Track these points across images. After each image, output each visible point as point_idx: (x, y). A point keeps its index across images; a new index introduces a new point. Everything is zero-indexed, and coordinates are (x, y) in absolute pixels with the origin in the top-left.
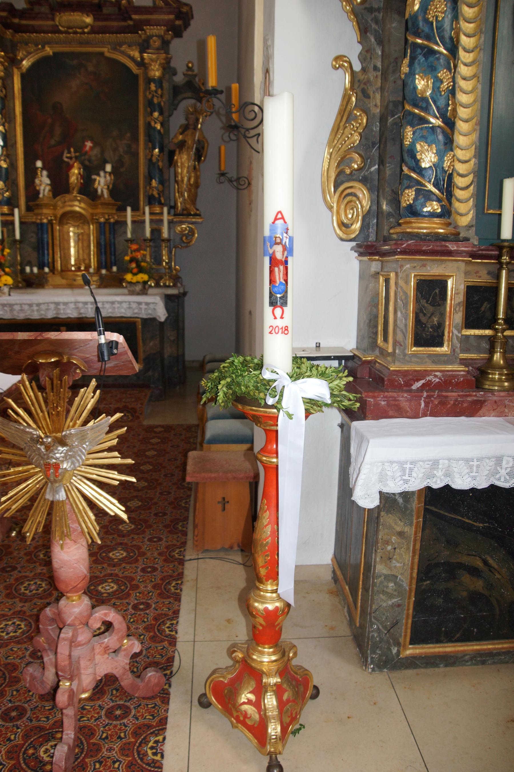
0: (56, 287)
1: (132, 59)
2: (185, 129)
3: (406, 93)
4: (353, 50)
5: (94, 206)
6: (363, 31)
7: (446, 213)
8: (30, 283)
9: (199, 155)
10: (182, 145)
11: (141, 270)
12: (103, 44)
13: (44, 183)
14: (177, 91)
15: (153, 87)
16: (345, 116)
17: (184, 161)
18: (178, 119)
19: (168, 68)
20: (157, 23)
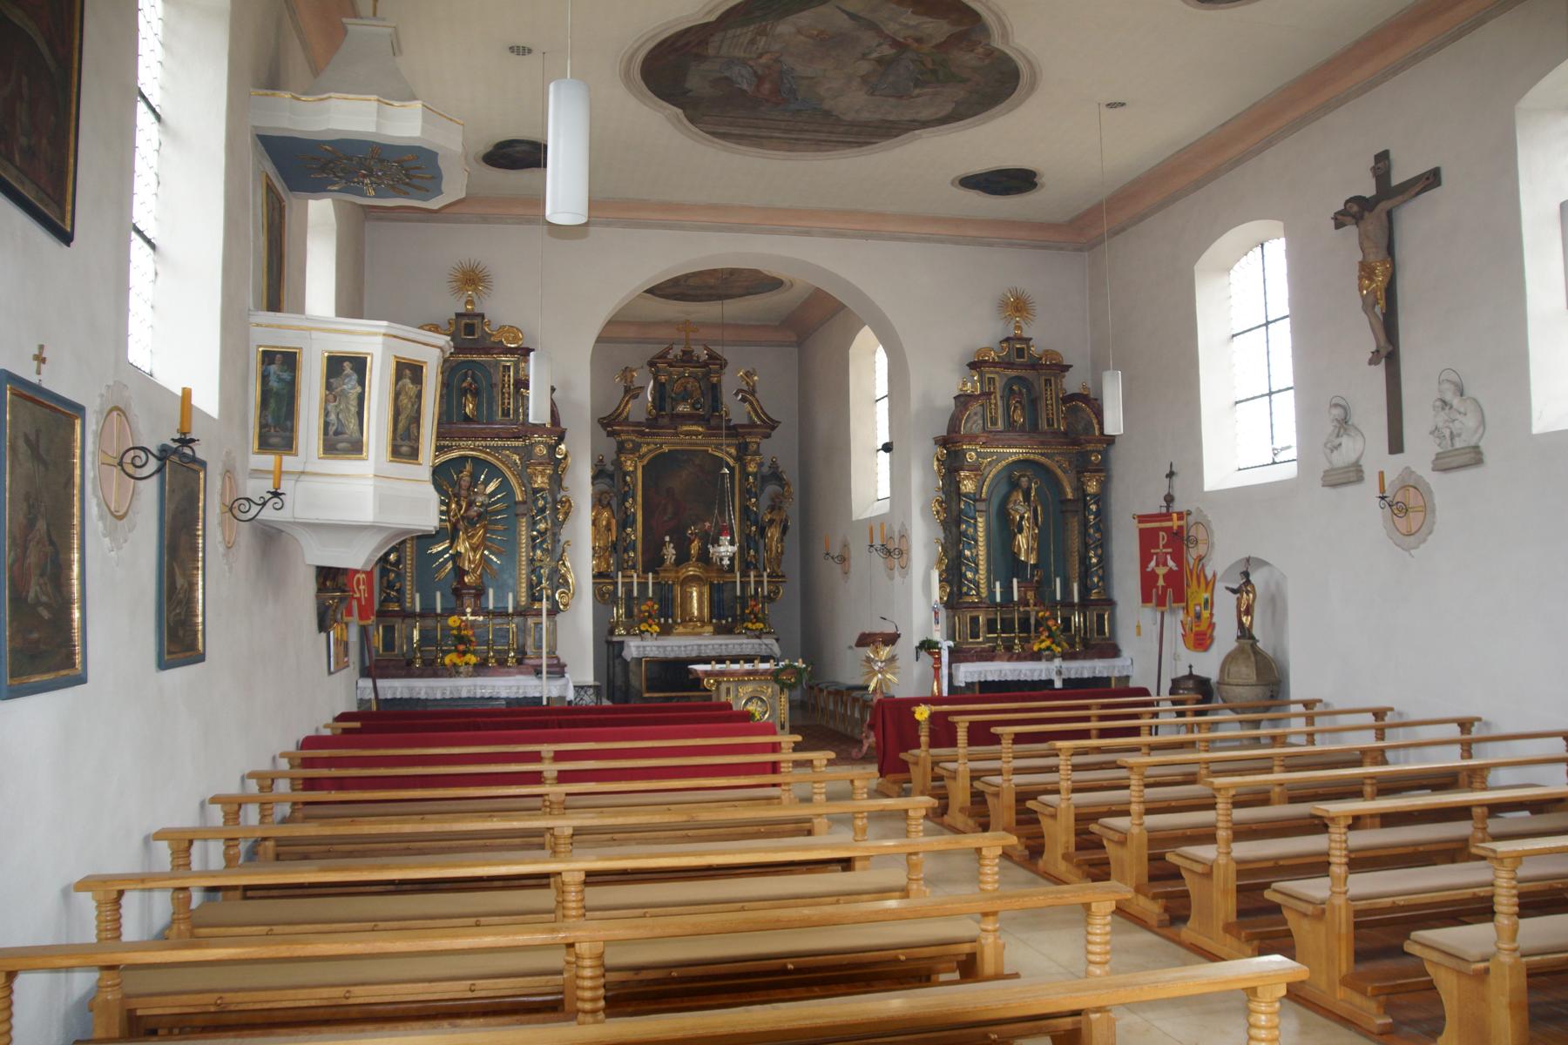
0: (679, 634)
1: (730, 455)
2: (772, 508)
3: (960, 554)
4: (941, 535)
5: (706, 571)
6: (945, 530)
7: (978, 594)
8: (666, 631)
9: (784, 530)
10: (772, 521)
11: (758, 620)
12: (708, 445)
13: (670, 553)
14: (764, 480)
15: (751, 479)
16: (940, 561)
17: (773, 533)
18: (765, 500)
19: (760, 465)
20: (756, 435)
